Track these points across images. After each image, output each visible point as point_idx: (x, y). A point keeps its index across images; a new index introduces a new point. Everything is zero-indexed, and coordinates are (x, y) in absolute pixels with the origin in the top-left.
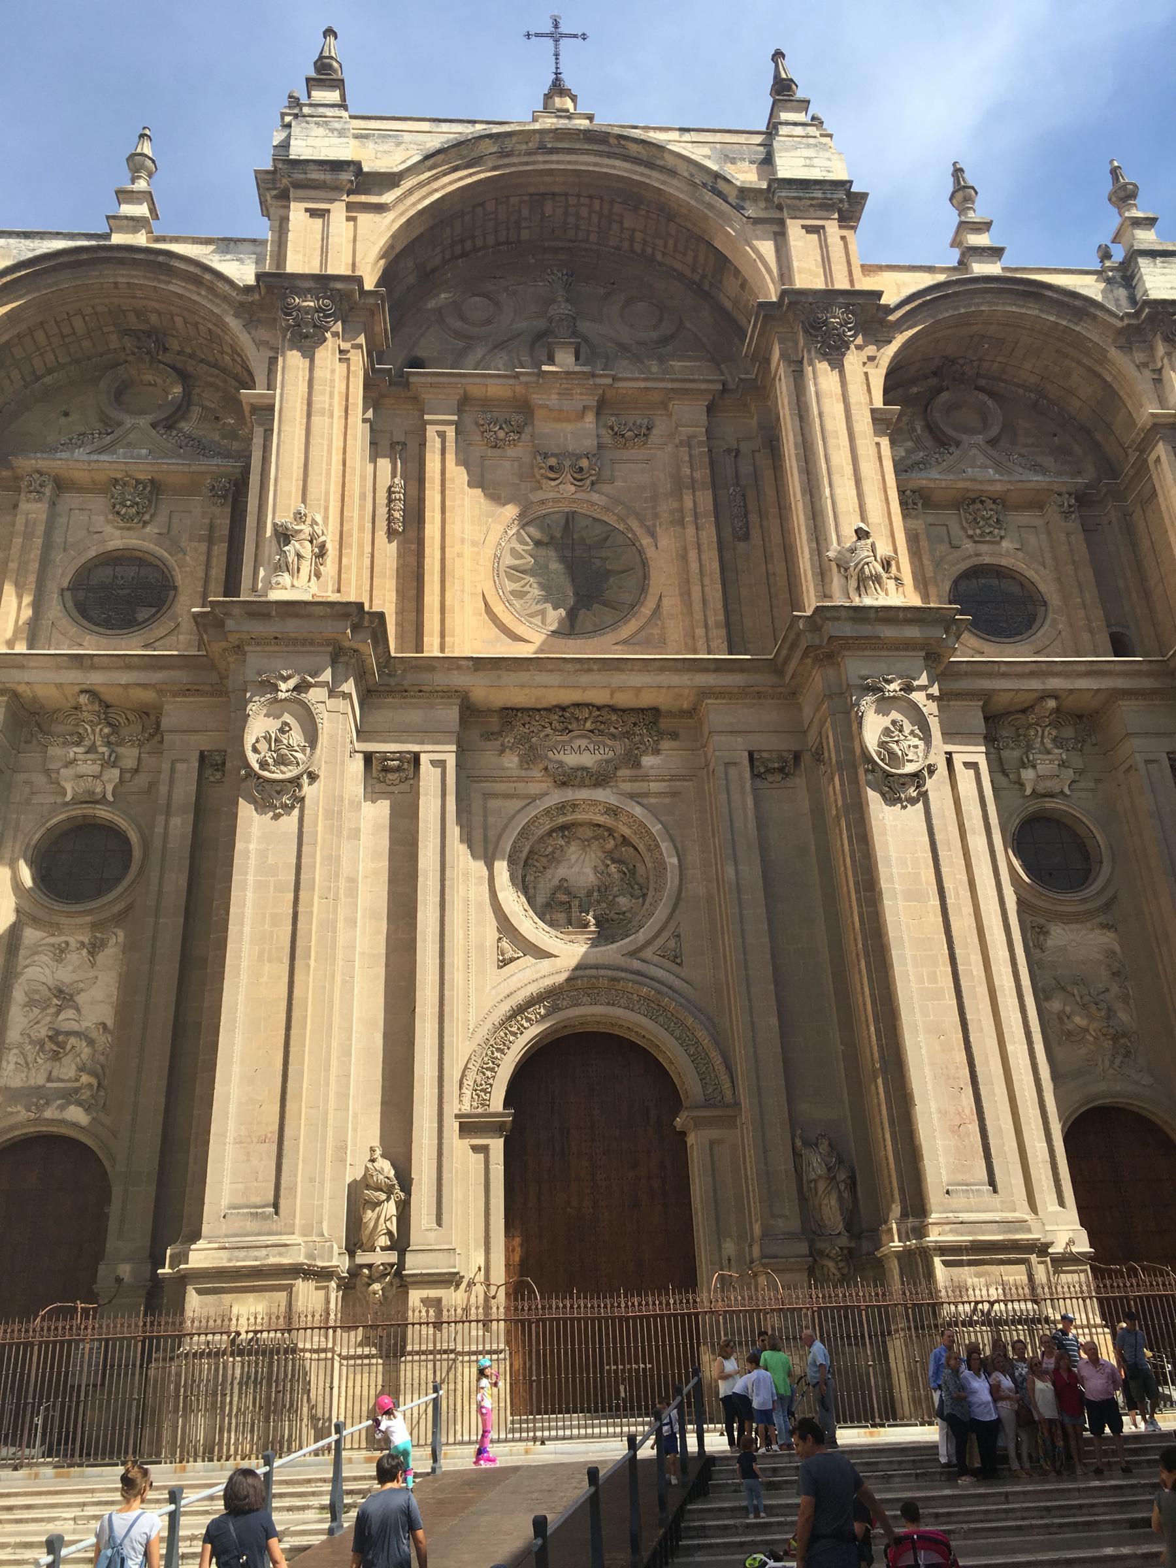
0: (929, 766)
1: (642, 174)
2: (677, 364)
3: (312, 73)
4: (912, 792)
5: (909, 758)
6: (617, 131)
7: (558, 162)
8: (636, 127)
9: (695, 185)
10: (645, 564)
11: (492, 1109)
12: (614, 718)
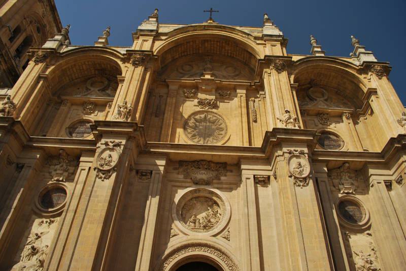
12: (213, 165)
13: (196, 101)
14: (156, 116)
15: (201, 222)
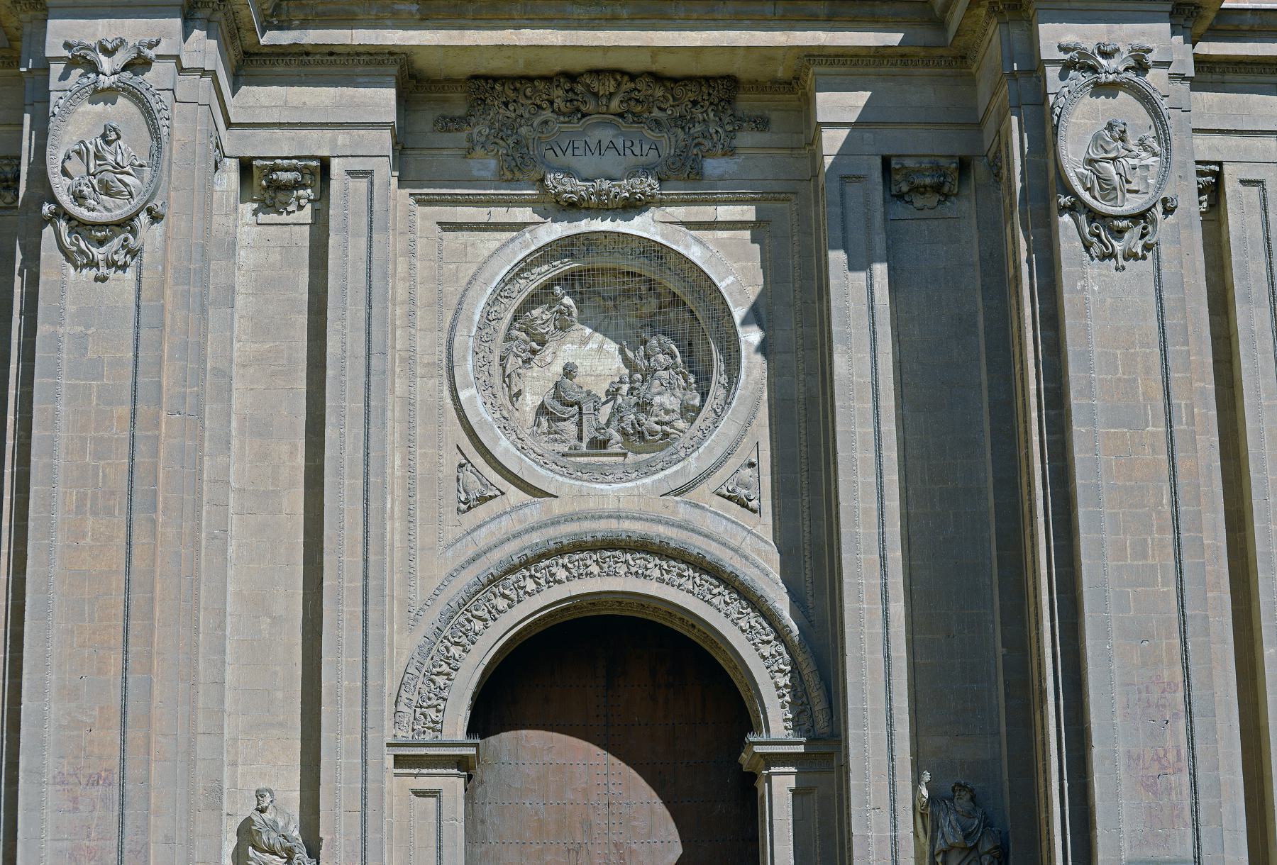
0: (1165, 201)
4: (1131, 239)
5: (1133, 187)
11: (445, 737)
12: (659, 92)
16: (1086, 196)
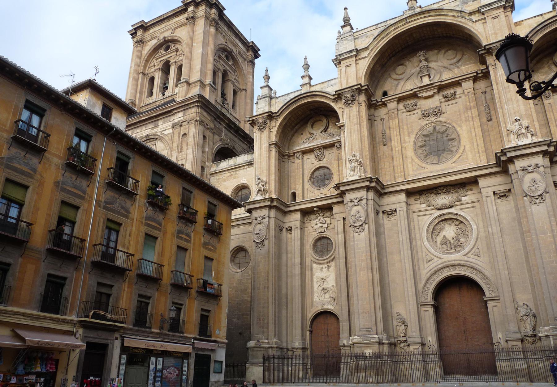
1: (438, 19)
2: (463, 68)
3: (343, 24)
6: (428, 8)
7: (412, 25)
8: (434, 4)
9: (454, 16)
10: (459, 136)
11: (428, 301)
13: (418, 111)
14: (385, 145)
15: (452, 241)
16: (529, 194)
